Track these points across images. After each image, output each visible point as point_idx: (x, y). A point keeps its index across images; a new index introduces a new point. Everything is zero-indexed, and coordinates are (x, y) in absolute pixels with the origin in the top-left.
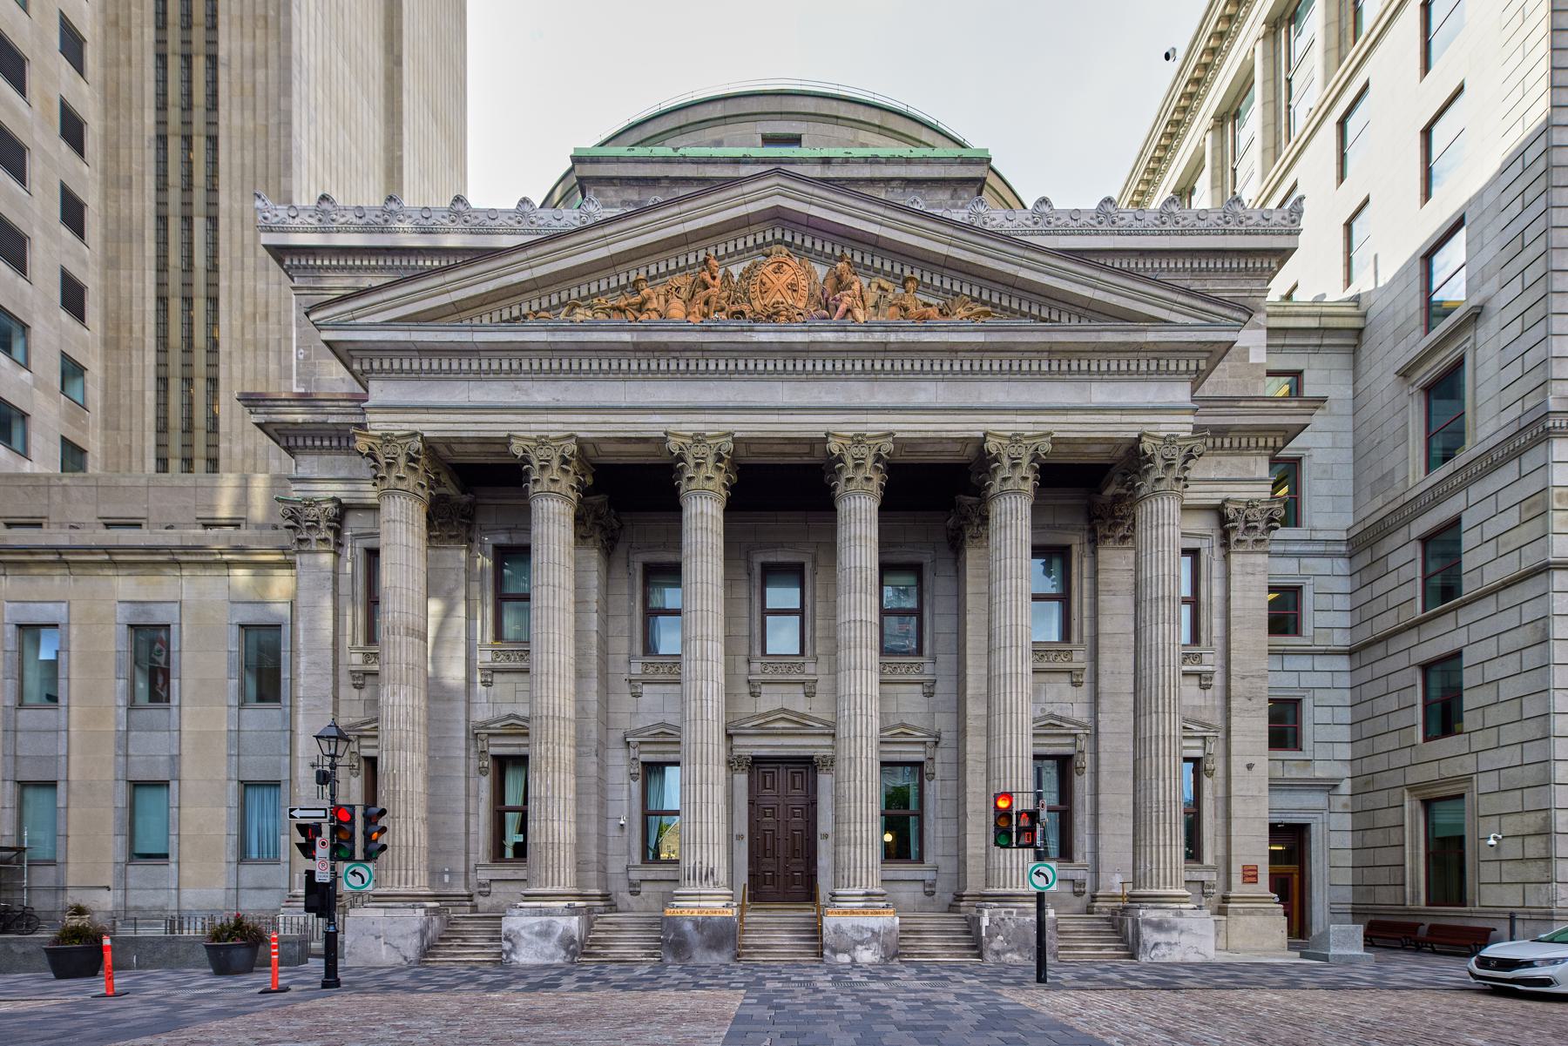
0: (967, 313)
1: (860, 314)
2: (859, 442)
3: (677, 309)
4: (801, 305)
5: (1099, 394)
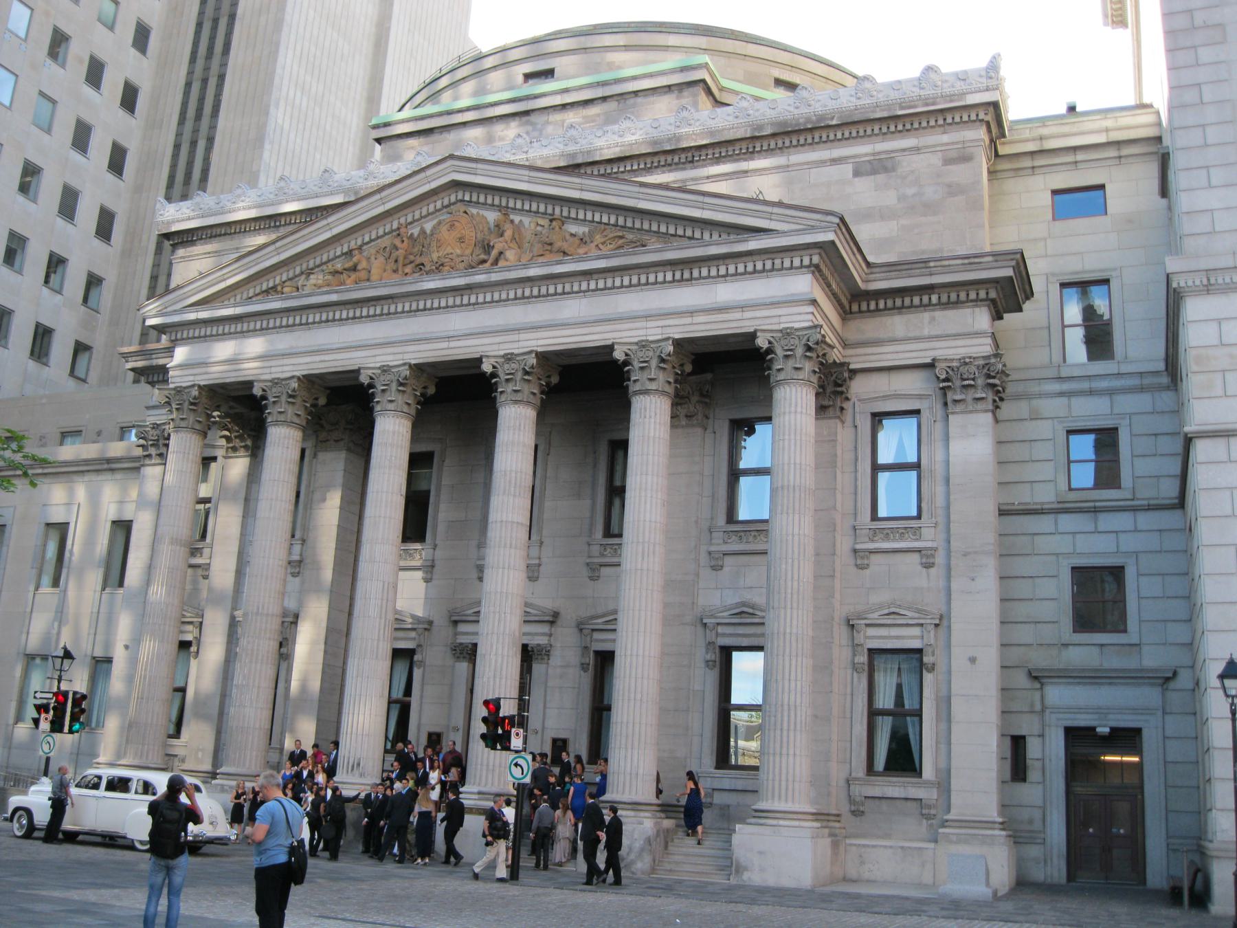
0: (603, 240)
1: (510, 255)
2: (509, 359)
3: (377, 265)
4: (468, 252)
5: (726, 292)
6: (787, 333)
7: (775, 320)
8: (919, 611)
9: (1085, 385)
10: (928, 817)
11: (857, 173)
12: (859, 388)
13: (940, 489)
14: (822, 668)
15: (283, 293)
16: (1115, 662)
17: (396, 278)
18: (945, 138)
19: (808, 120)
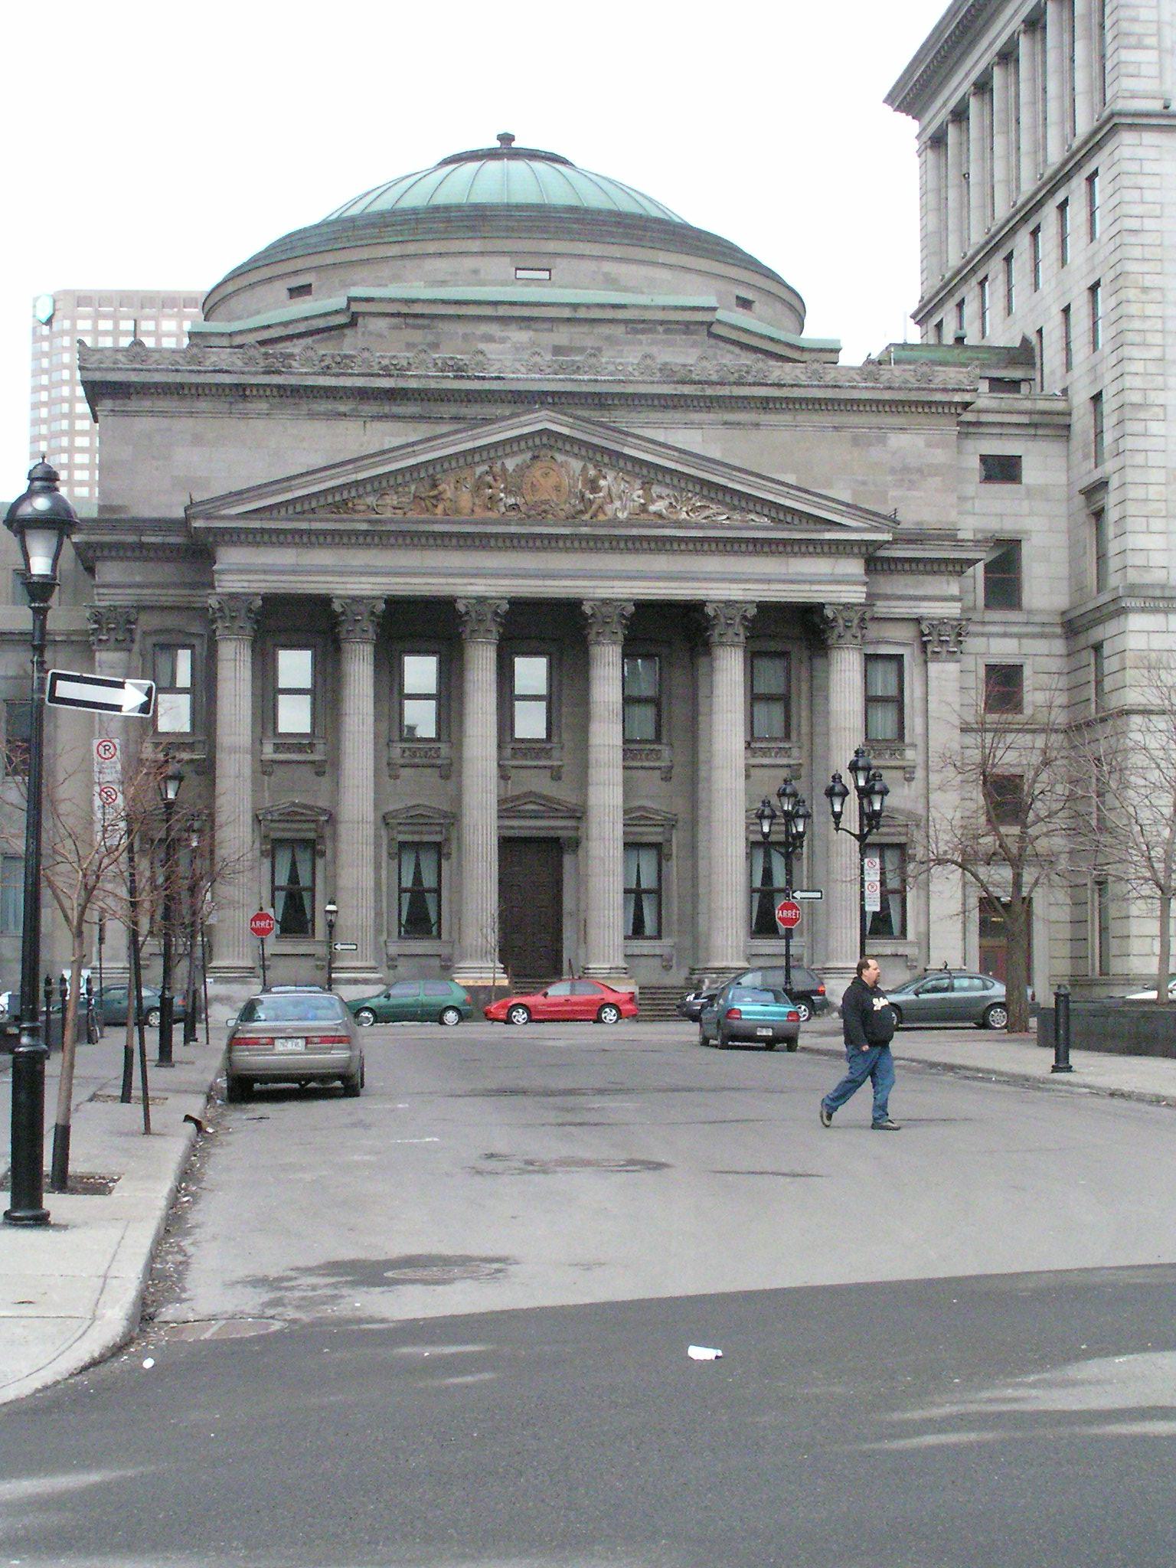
6: (848, 606)
7: (837, 594)
15: (355, 511)
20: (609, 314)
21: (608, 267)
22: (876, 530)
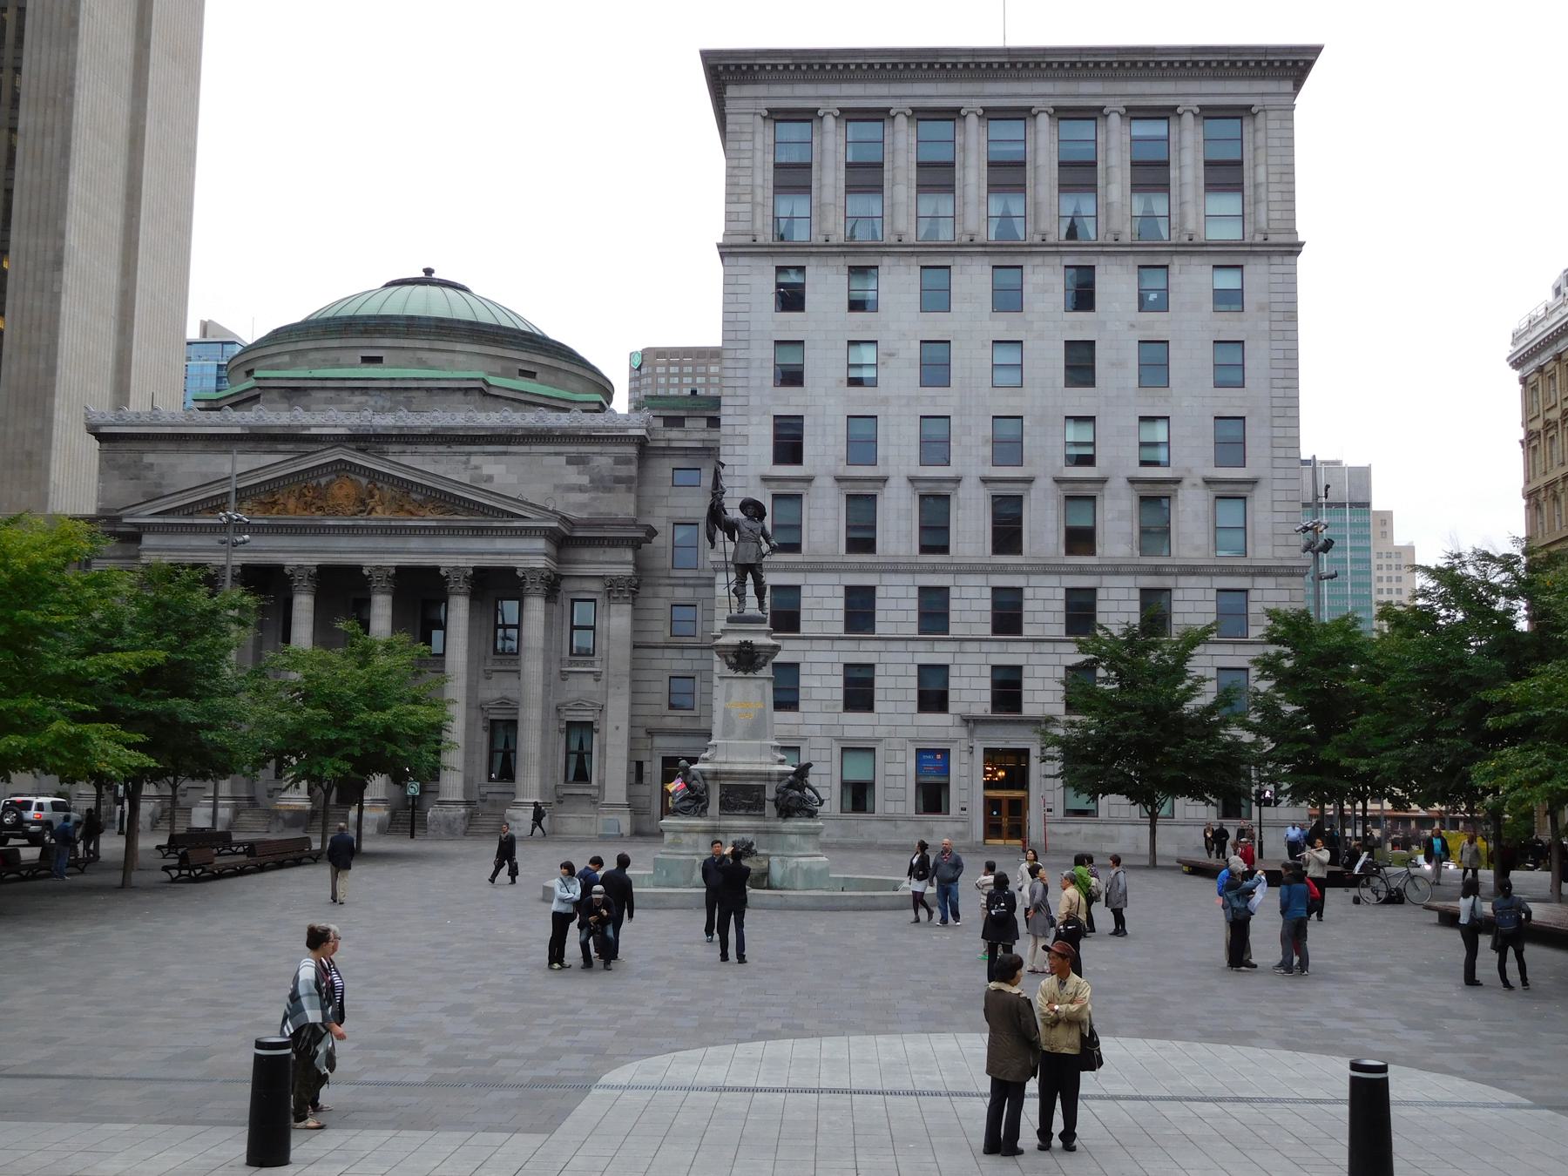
1: (379, 509)
3: (292, 503)
5: (500, 544)
6: (533, 569)
8: (592, 703)
9: (682, 582)
10: (595, 803)
11: (570, 462)
12: (566, 585)
13: (605, 642)
14: (545, 732)
16: (688, 725)
17: (305, 513)
18: (617, 449)
19: (542, 429)
20: (414, 384)
21: (420, 354)
22: (548, 520)
